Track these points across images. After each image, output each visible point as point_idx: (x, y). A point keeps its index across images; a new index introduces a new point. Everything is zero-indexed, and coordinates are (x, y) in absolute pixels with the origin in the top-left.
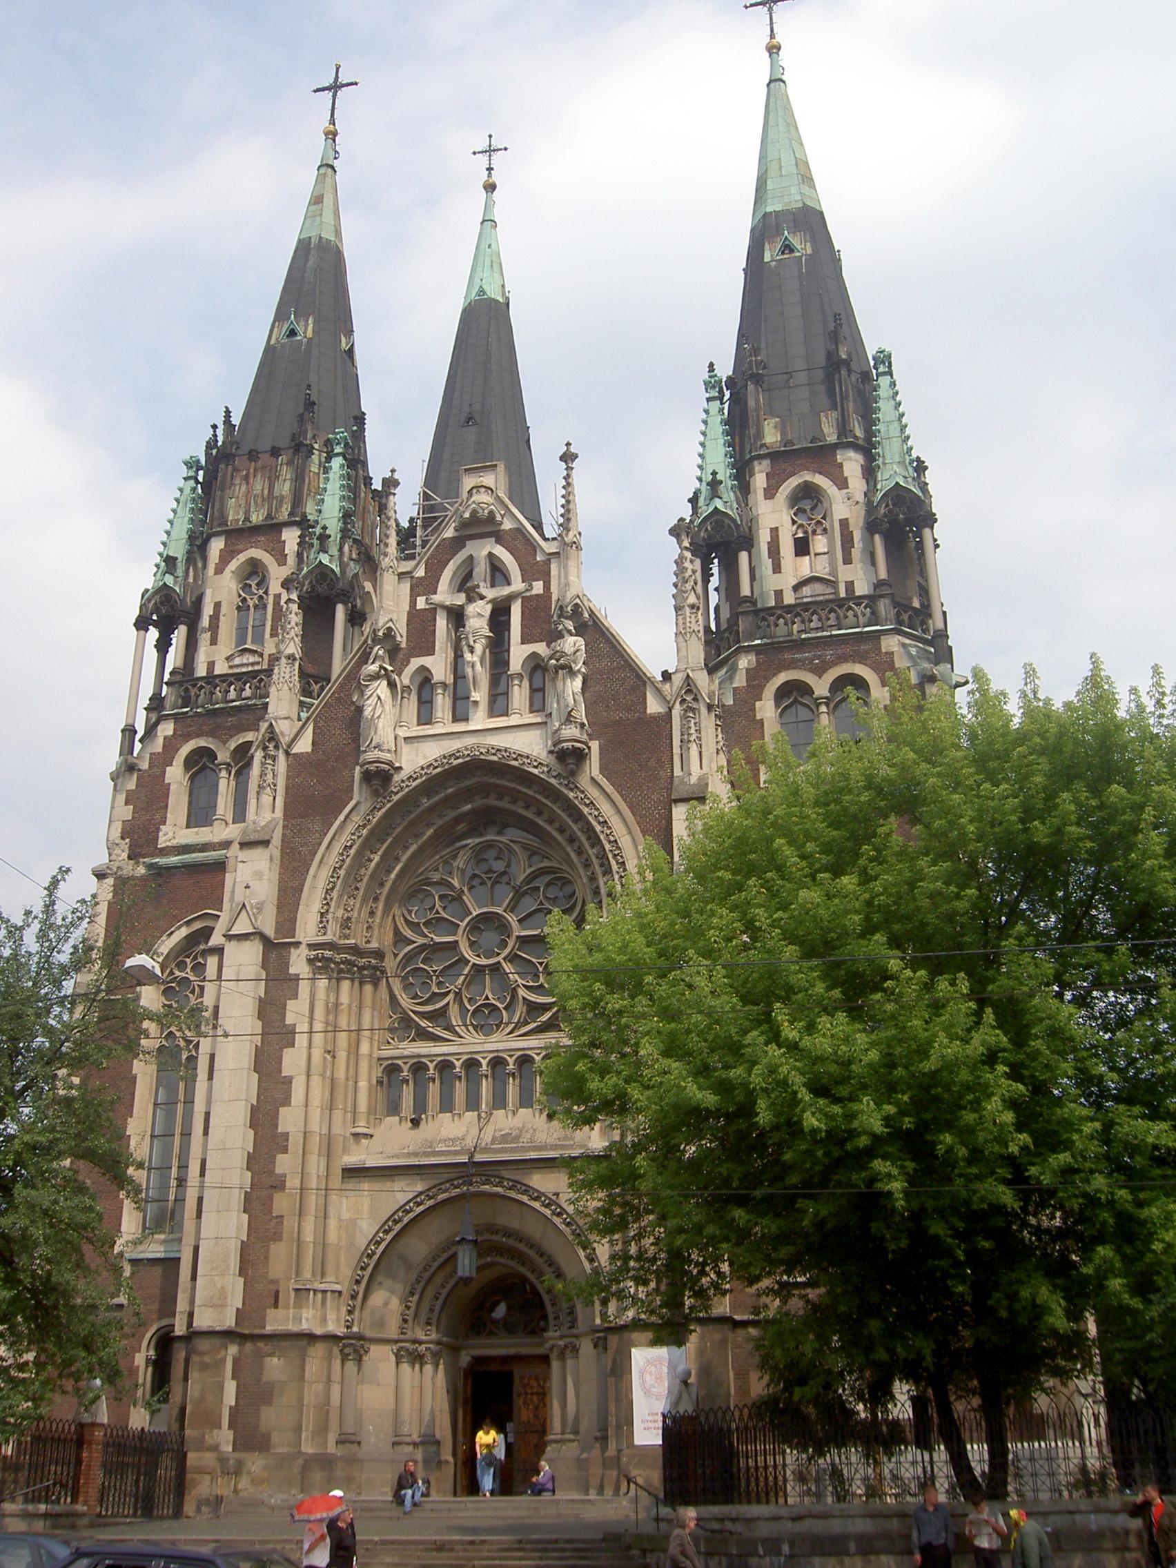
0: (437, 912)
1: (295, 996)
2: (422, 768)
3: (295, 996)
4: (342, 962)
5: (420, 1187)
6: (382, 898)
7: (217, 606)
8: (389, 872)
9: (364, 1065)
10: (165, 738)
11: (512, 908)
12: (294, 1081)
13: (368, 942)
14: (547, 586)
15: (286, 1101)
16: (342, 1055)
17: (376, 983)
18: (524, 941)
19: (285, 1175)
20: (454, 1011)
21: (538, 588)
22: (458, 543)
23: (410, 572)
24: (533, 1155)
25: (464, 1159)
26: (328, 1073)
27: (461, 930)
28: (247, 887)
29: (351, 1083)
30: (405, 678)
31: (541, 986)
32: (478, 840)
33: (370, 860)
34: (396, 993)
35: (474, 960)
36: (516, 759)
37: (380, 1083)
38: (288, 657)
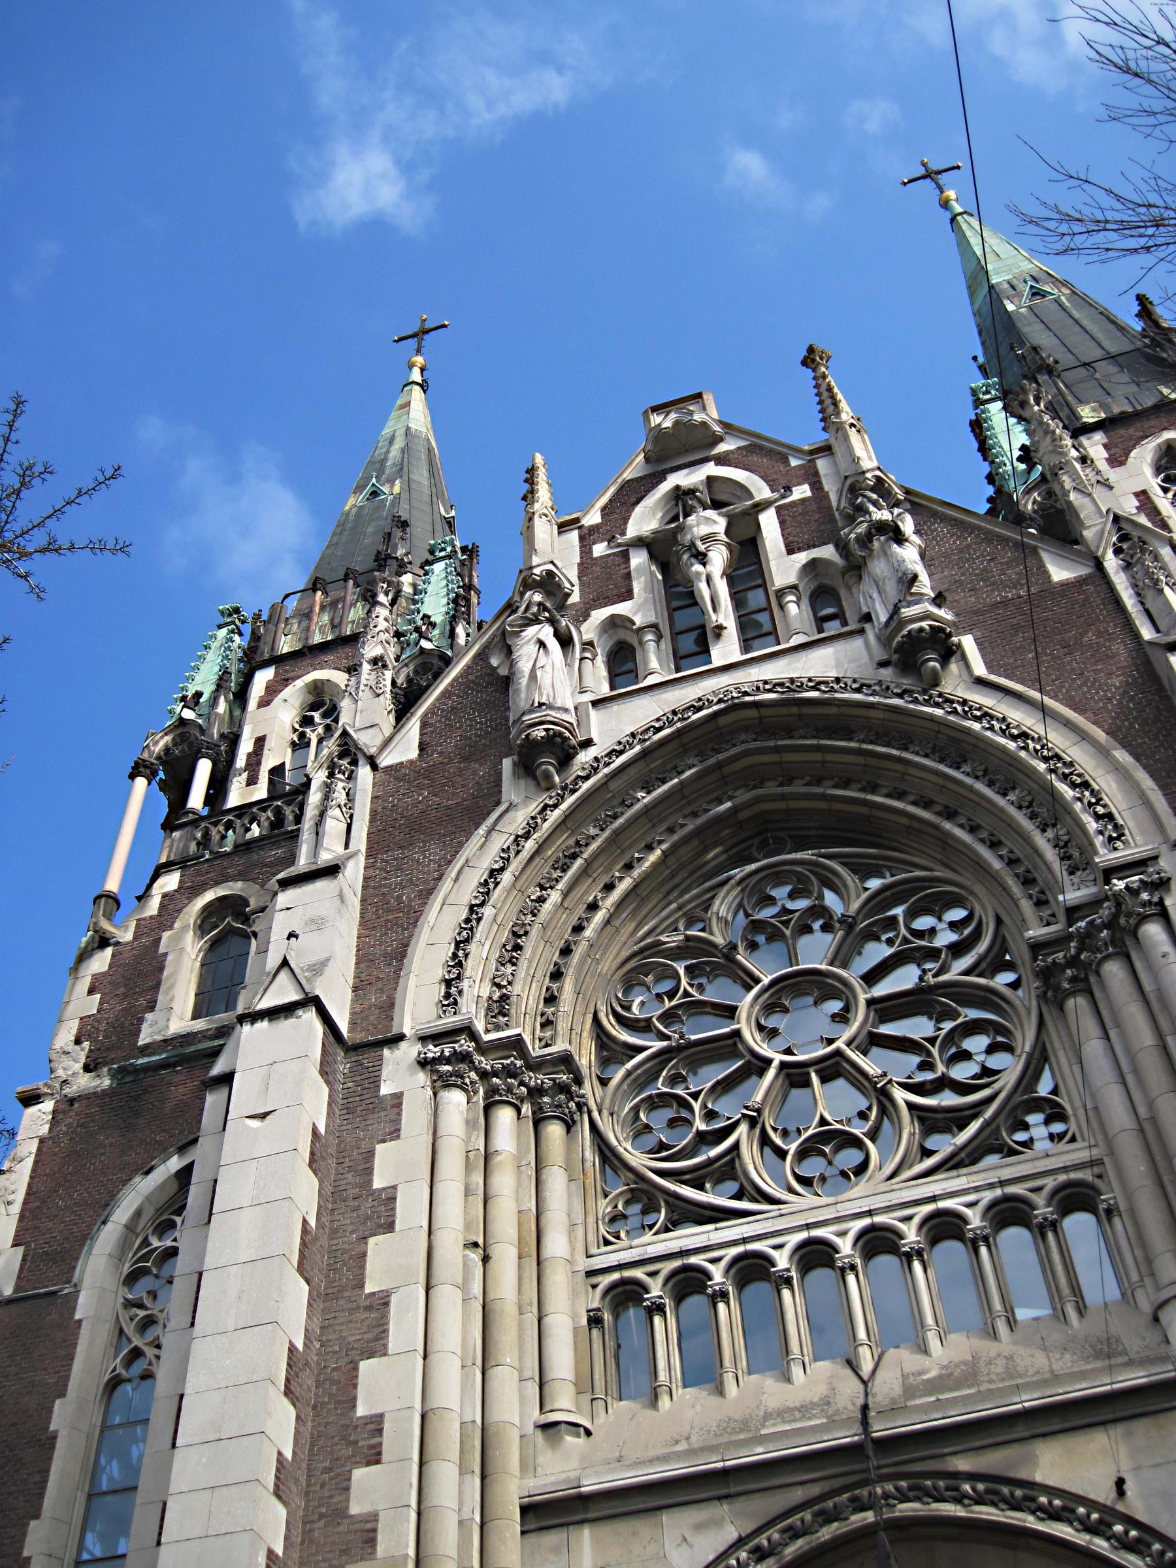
0: (686, 994)
1: (395, 1134)
2: (633, 735)
3: (395, 1134)
4: (495, 1074)
5: (731, 1533)
6: (571, 971)
7: (260, 742)
8: (578, 929)
9: (560, 1284)
10: (165, 896)
11: (842, 957)
12: (394, 1299)
13: (547, 1045)
14: (816, 486)
15: (376, 1346)
16: (506, 1255)
17: (569, 1126)
18: (887, 1008)
19: (374, 1517)
20: (751, 1158)
21: (802, 492)
22: (655, 479)
23: (577, 520)
24: (1029, 1400)
25: (846, 1437)
26: (477, 1289)
27: (743, 1013)
28: (292, 935)
29: (531, 1317)
30: (589, 629)
31: (943, 1083)
32: (753, 866)
33: (541, 900)
34: (614, 1142)
35: (778, 1058)
36: (814, 688)
37: (595, 1320)
38: (375, 661)
